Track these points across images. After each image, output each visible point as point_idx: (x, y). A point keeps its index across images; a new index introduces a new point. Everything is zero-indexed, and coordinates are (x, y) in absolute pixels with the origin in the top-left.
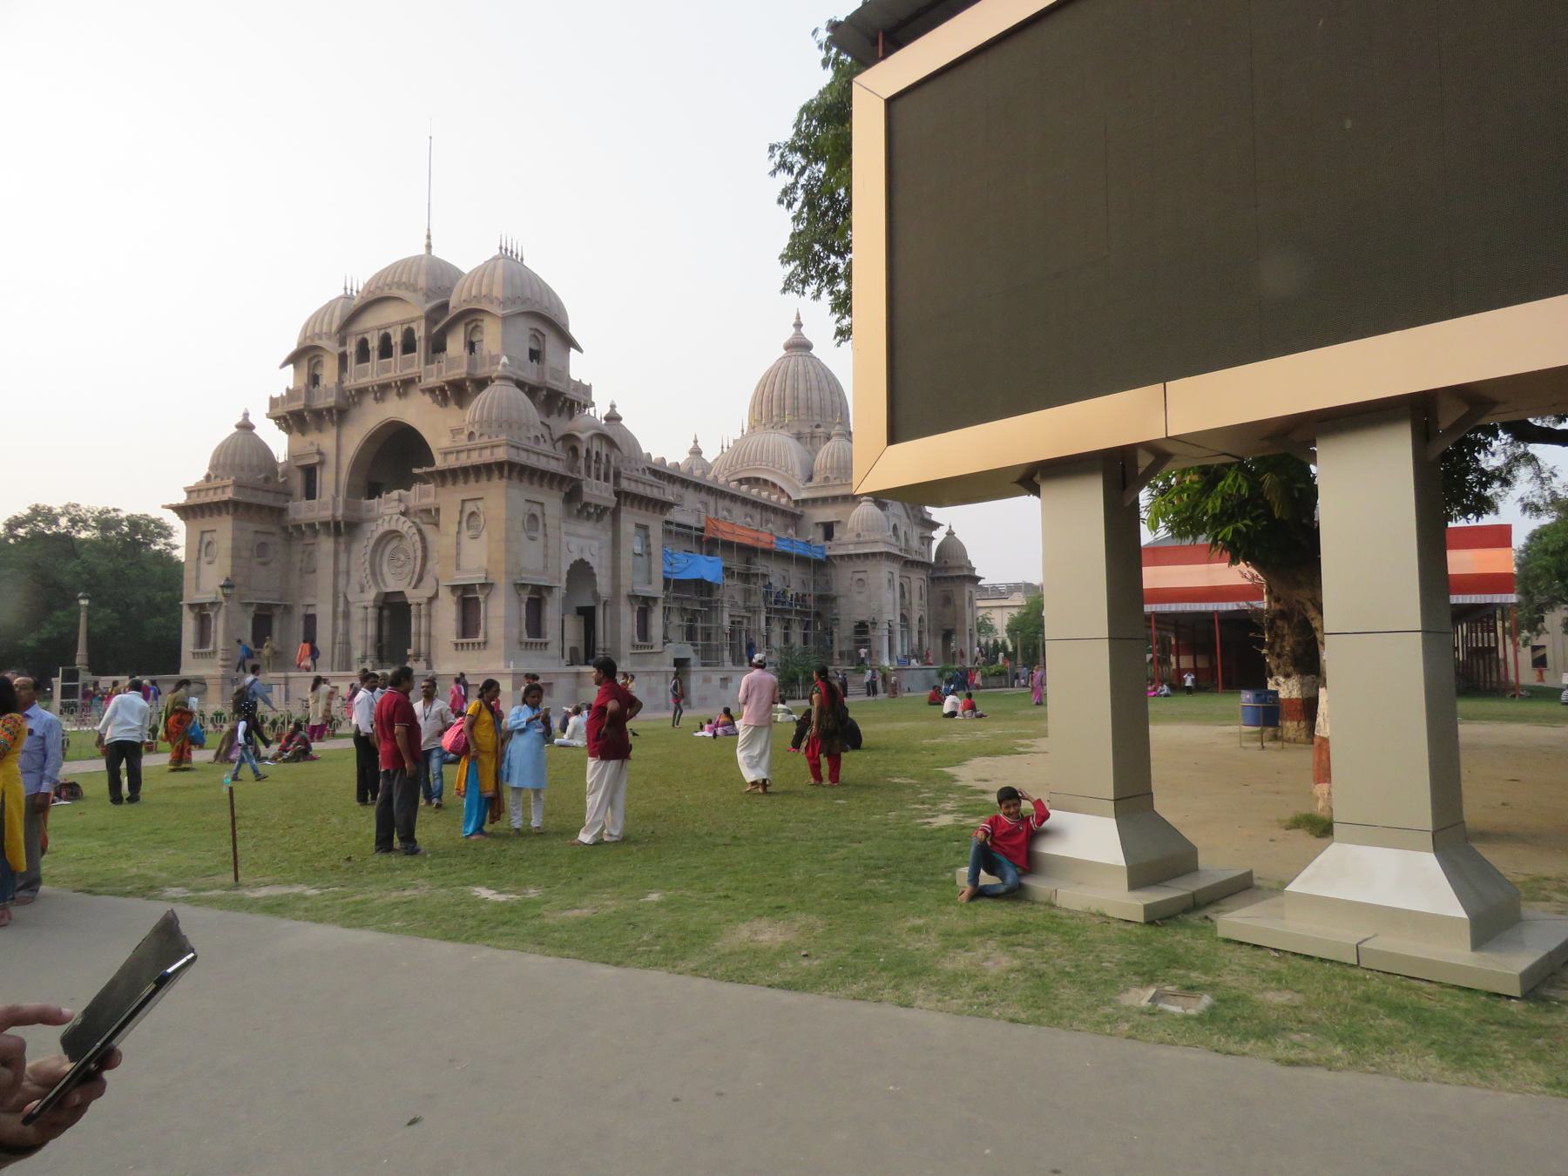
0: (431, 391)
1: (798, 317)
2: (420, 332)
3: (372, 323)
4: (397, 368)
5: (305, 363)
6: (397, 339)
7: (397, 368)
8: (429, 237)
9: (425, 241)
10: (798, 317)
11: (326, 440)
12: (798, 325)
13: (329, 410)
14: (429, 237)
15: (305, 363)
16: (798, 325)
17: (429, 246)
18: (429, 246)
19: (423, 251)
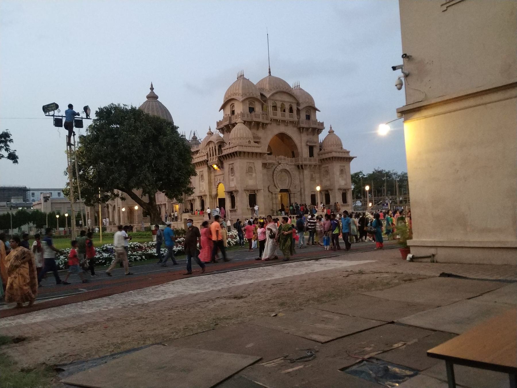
0: (303, 128)
1: (152, 85)
2: (295, 108)
3: (278, 97)
4: (287, 116)
5: (247, 102)
6: (287, 107)
7: (287, 116)
8: (270, 69)
9: (268, 71)
10: (152, 85)
11: (260, 133)
12: (152, 89)
13: (267, 124)
14: (270, 69)
15: (247, 102)
16: (152, 89)
17: (270, 72)
18: (270, 72)
19: (268, 74)
